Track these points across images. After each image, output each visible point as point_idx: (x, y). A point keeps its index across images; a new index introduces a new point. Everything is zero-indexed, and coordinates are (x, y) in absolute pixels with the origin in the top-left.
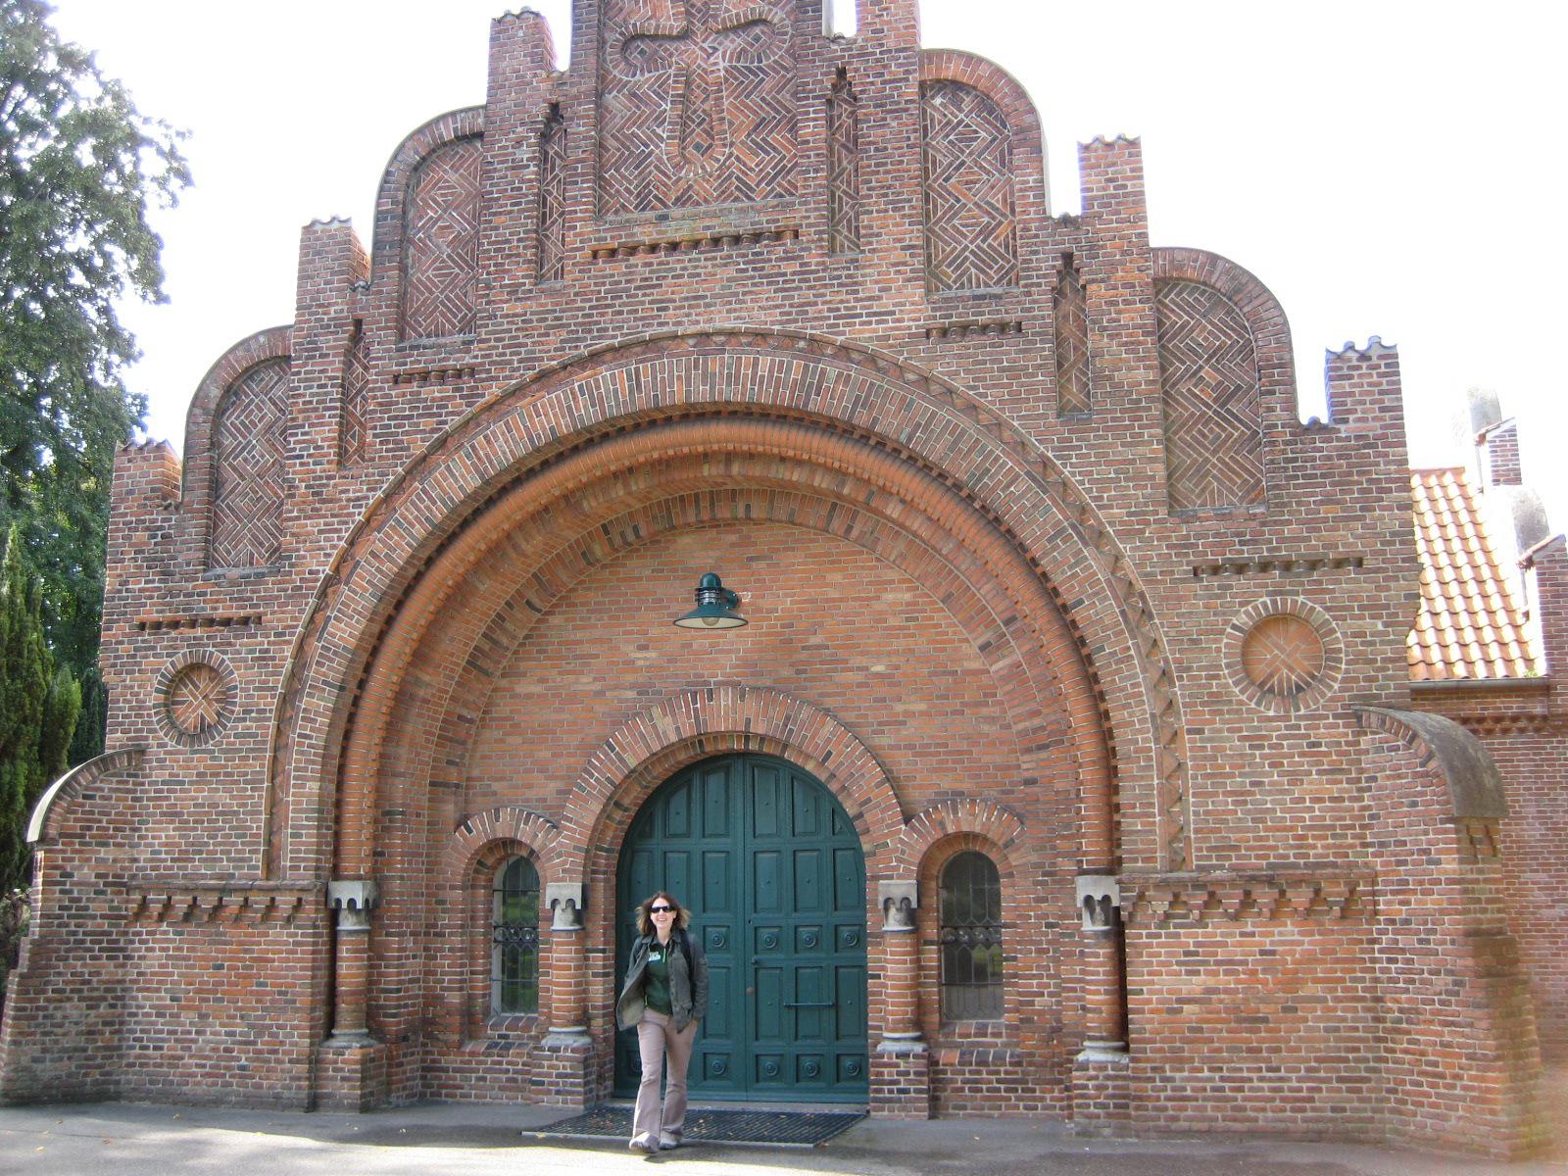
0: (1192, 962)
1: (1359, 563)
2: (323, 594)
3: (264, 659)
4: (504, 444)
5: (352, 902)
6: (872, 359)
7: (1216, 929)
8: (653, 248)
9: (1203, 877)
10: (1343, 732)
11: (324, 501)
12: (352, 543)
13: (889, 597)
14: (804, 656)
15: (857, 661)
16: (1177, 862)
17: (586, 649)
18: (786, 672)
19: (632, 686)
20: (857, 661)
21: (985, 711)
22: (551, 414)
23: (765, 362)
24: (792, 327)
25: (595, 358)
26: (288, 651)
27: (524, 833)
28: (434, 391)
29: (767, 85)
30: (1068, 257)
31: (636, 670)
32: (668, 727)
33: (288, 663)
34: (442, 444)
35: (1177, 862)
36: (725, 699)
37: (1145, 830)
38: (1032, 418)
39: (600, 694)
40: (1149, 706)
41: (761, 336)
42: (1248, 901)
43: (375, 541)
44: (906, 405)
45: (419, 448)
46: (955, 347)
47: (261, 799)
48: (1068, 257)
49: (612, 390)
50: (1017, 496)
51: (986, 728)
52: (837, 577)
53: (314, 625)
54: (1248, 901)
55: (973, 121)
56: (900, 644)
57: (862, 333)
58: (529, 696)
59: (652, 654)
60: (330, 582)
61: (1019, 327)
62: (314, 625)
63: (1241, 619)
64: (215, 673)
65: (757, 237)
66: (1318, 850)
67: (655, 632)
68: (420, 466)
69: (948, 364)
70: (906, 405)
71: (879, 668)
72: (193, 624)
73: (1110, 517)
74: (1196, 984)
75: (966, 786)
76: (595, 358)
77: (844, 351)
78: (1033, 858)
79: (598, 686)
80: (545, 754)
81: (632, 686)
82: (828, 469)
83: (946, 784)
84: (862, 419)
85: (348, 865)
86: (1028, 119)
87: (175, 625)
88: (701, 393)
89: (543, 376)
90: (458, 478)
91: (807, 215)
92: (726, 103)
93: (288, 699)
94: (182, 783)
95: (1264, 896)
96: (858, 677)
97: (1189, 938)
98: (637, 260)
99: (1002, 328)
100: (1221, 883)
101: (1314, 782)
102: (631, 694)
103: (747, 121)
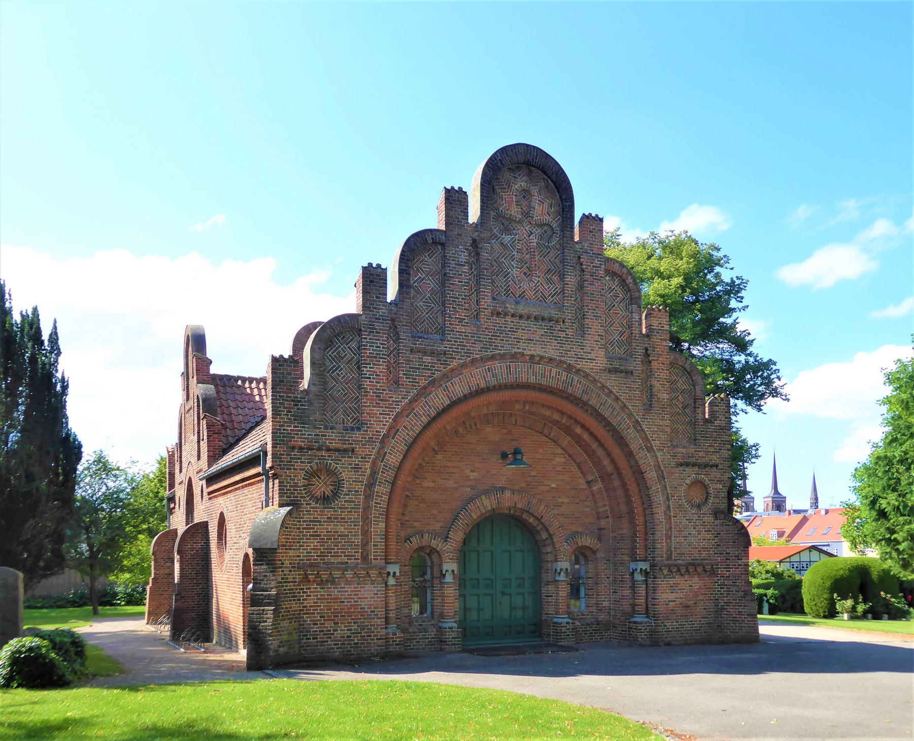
0: (673, 588)
1: (717, 466)
2: (382, 442)
3: (356, 468)
4: (459, 387)
5: (394, 573)
6: (587, 376)
7: (678, 579)
8: (513, 316)
9: (676, 562)
10: (711, 519)
11: (381, 400)
12: (395, 420)
13: (557, 459)
14: (530, 479)
15: (547, 482)
16: (669, 557)
17: (451, 470)
18: (524, 485)
19: (469, 486)
20: (547, 482)
21: (586, 503)
22: (477, 377)
23: (554, 370)
24: (563, 359)
25: (493, 358)
26: (368, 465)
27: (434, 543)
28: (428, 359)
29: (551, 254)
30: (647, 350)
31: (470, 480)
32: (487, 503)
33: (369, 471)
34: (432, 383)
35: (669, 557)
36: (508, 494)
37: (661, 547)
38: (636, 407)
39: (456, 489)
40: (663, 508)
41: (551, 360)
42: (687, 570)
43: (405, 421)
44: (598, 395)
45: (423, 383)
46: (613, 377)
47: (358, 529)
48: (647, 350)
49: (500, 371)
50: (630, 434)
51: (586, 510)
52: (541, 451)
53: (381, 455)
54: (687, 570)
55: (618, 289)
56: (560, 477)
57: (585, 366)
58: (428, 487)
59: (476, 474)
60: (386, 436)
61: (632, 373)
62: (381, 455)
63: (688, 482)
64: (331, 472)
65: (550, 320)
66: (704, 554)
67: (477, 465)
68: (424, 392)
69: (612, 382)
70: (598, 395)
71: (554, 486)
72: (319, 449)
73: (656, 444)
74: (673, 596)
75: (580, 530)
76: (493, 358)
77: (578, 371)
78: (603, 555)
79: (455, 485)
80: (435, 512)
81: (469, 486)
82: (559, 411)
83: (574, 528)
84: (585, 398)
85: (393, 558)
86: (637, 294)
87: (310, 448)
88: (532, 380)
89: (474, 361)
90: (439, 398)
91: (568, 315)
92: (537, 258)
93: (370, 485)
94: (320, 522)
95: (691, 569)
96: (547, 488)
97: (672, 581)
98: (509, 319)
99: (627, 372)
100: (680, 565)
101: (704, 534)
102: (469, 489)
103: (544, 267)
